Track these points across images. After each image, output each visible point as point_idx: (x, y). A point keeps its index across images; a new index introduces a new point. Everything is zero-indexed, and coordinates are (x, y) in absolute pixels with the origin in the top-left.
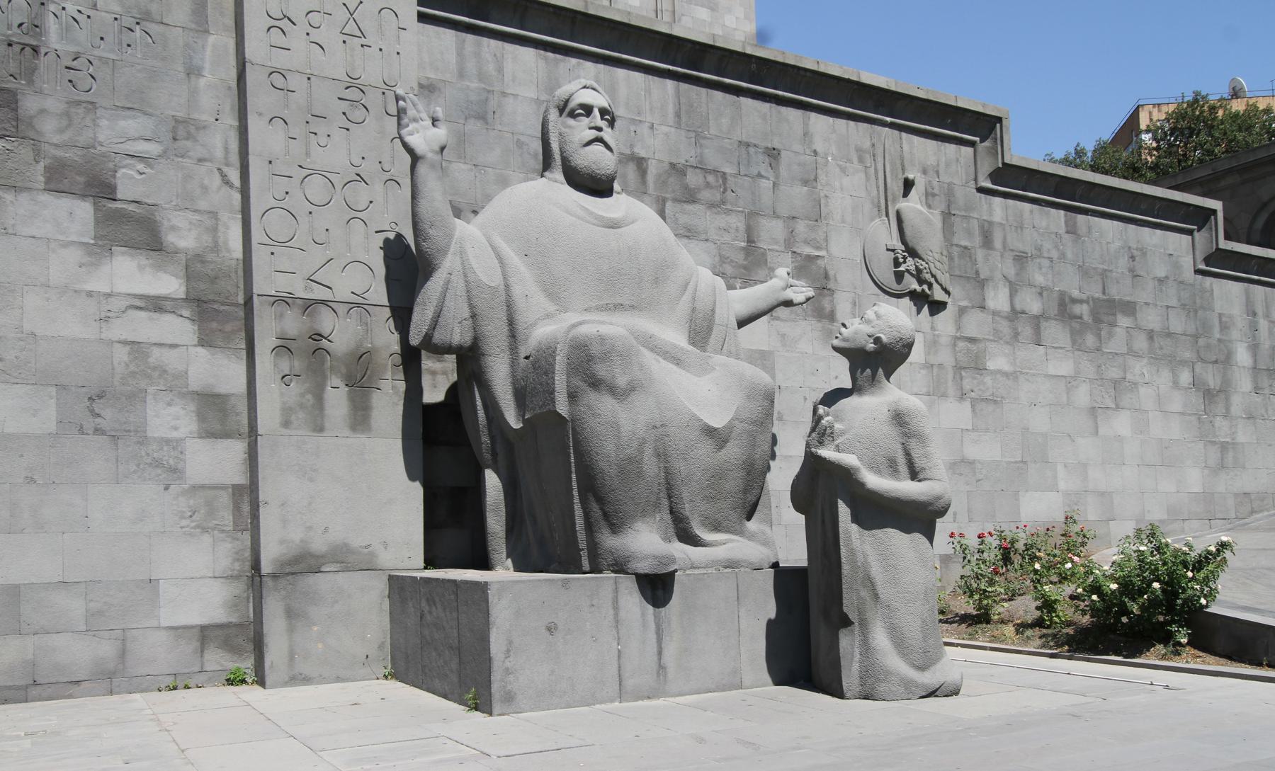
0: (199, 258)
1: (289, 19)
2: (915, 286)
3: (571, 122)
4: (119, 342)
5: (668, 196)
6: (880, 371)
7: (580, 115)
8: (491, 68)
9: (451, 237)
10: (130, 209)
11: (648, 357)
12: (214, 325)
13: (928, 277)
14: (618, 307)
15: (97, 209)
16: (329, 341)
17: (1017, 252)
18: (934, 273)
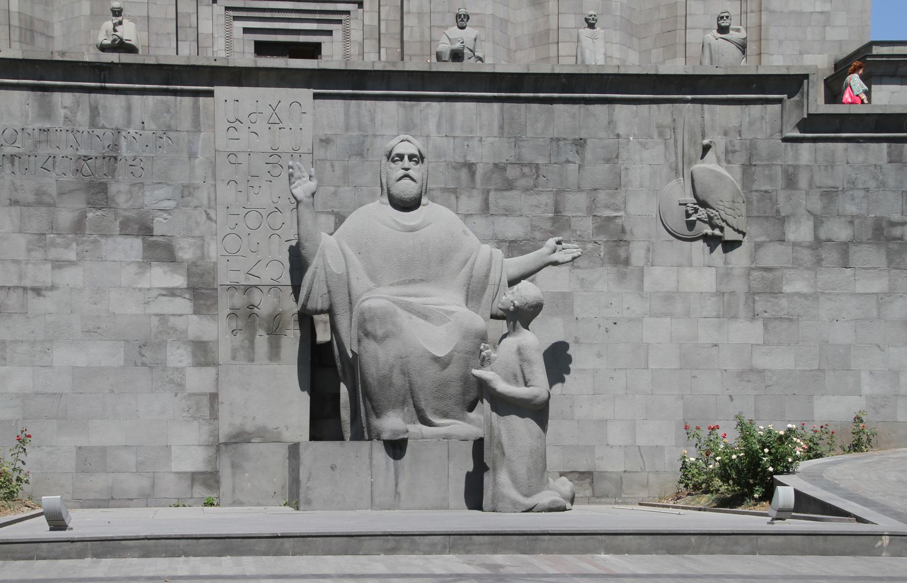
0: (194, 264)
1: (239, 121)
2: (709, 231)
3: (393, 165)
4: (154, 315)
5: (492, 187)
6: (518, 323)
7: (397, 160)
8: (366, 121)
9: (317, 246)
10: (160, 240)
11: (404, 318)
12: (202, 302)
13: (719, 222)
14: (412, 281)
15: (144, 241)
16: (258, 309)
17: (825, 188)
18: (724, 218)
